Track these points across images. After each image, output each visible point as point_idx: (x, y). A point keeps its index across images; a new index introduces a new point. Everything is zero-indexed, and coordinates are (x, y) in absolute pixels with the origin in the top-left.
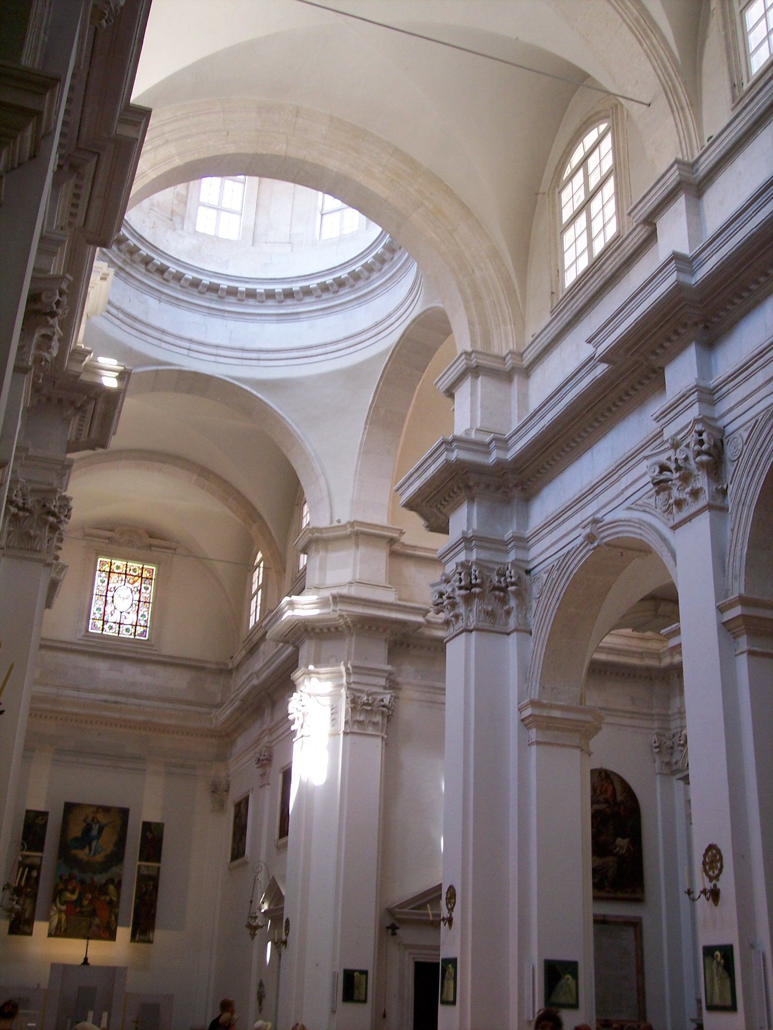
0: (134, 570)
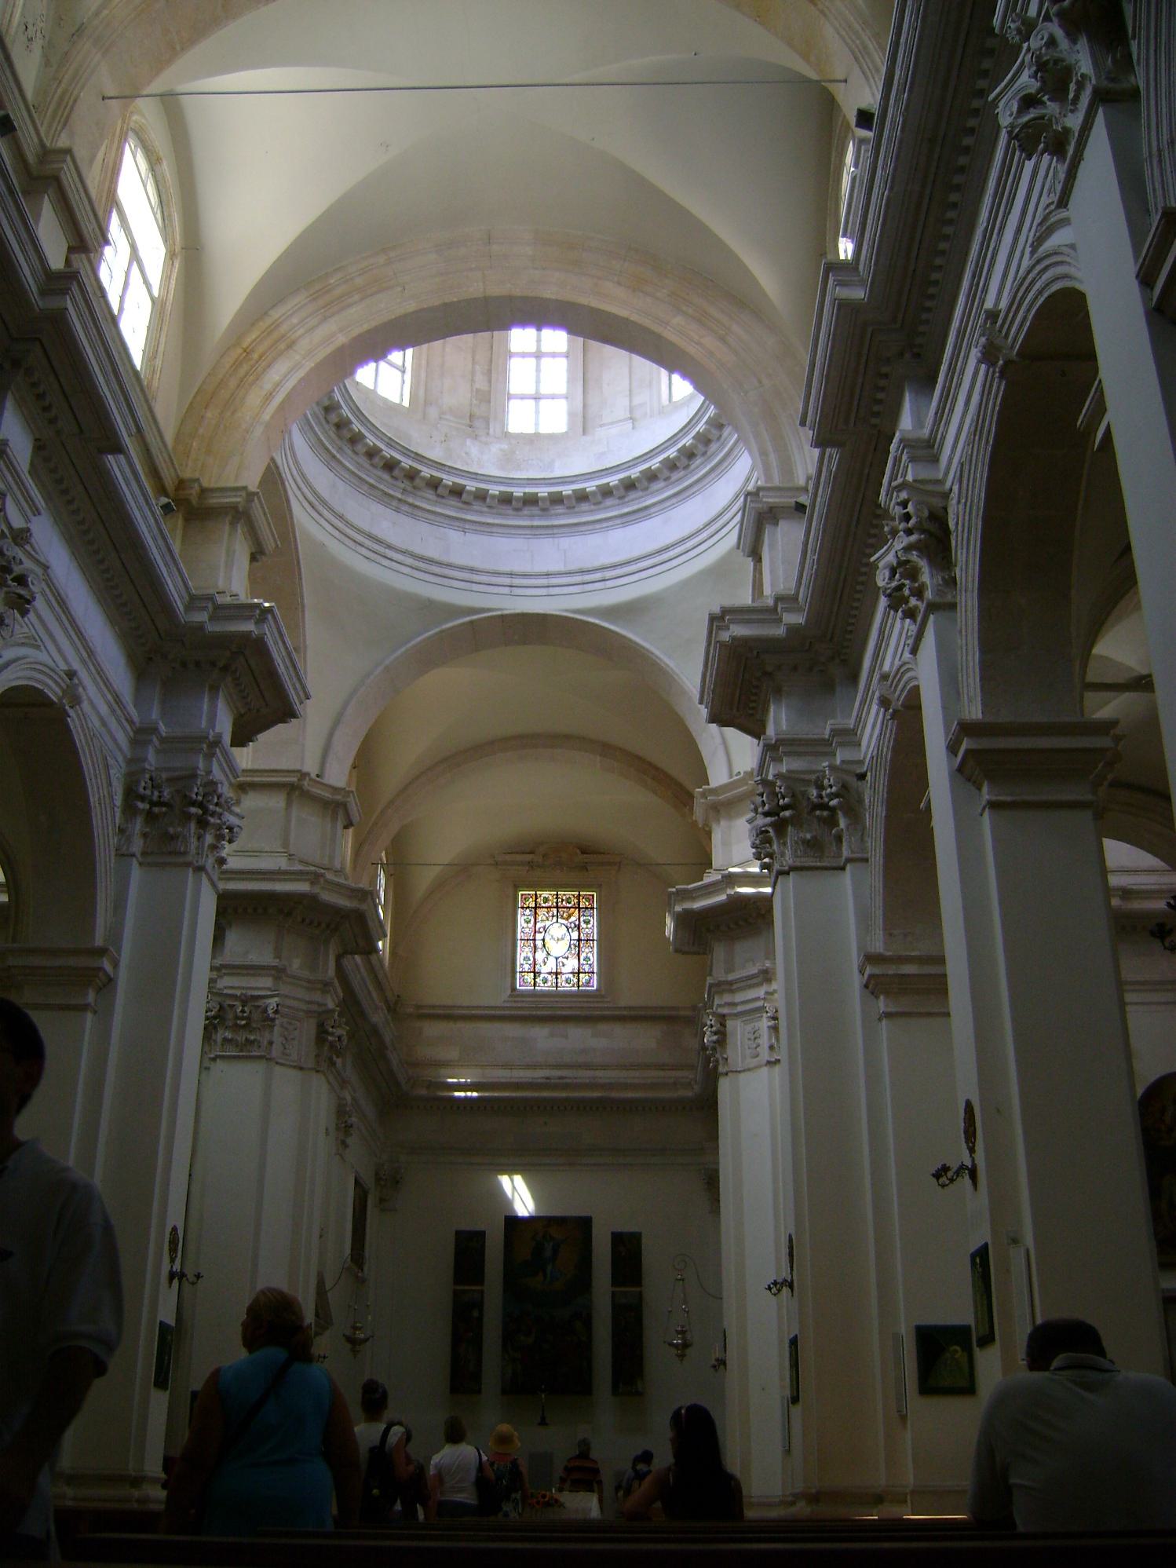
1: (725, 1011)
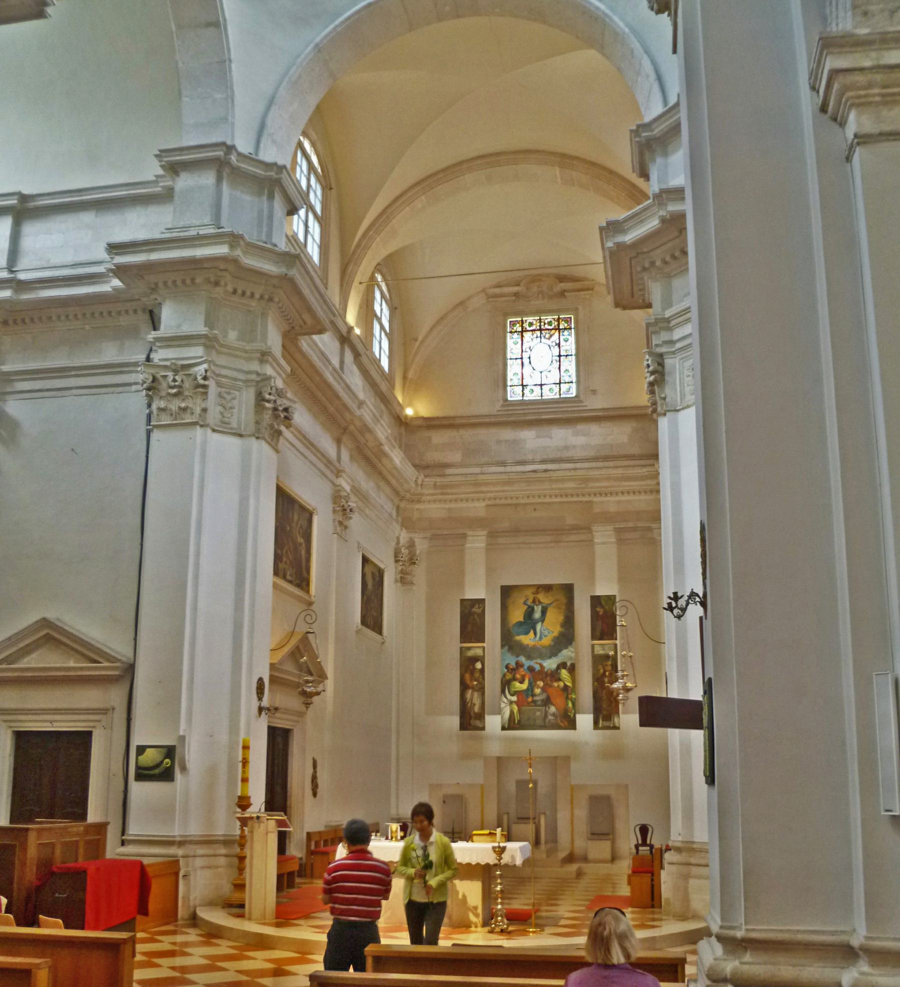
0: (550, 323)
1: (663, 350)
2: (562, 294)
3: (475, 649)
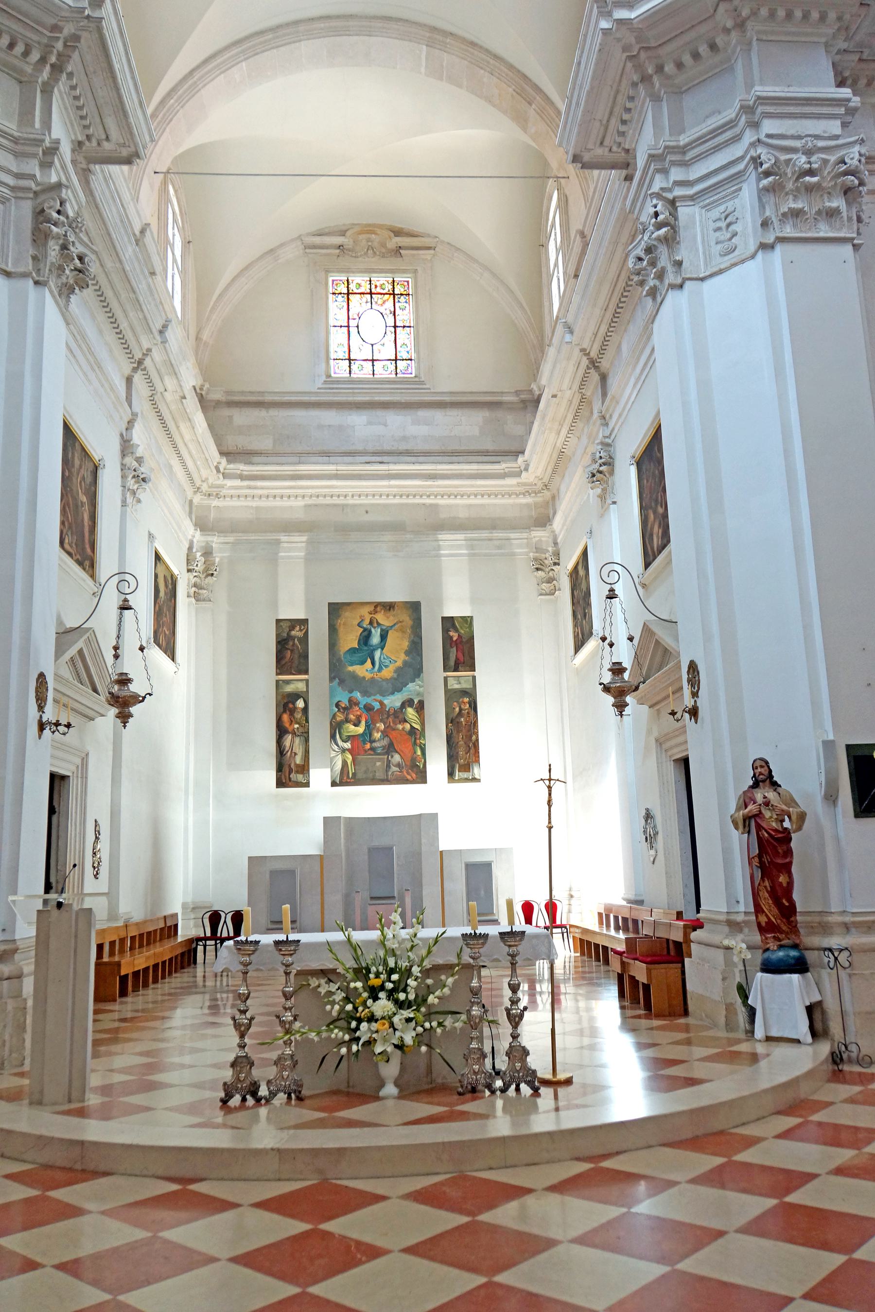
2: (398, 251)
3: (296, 683)
